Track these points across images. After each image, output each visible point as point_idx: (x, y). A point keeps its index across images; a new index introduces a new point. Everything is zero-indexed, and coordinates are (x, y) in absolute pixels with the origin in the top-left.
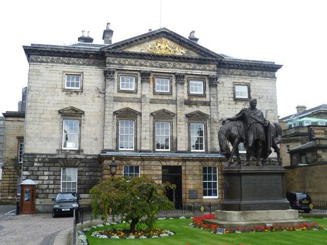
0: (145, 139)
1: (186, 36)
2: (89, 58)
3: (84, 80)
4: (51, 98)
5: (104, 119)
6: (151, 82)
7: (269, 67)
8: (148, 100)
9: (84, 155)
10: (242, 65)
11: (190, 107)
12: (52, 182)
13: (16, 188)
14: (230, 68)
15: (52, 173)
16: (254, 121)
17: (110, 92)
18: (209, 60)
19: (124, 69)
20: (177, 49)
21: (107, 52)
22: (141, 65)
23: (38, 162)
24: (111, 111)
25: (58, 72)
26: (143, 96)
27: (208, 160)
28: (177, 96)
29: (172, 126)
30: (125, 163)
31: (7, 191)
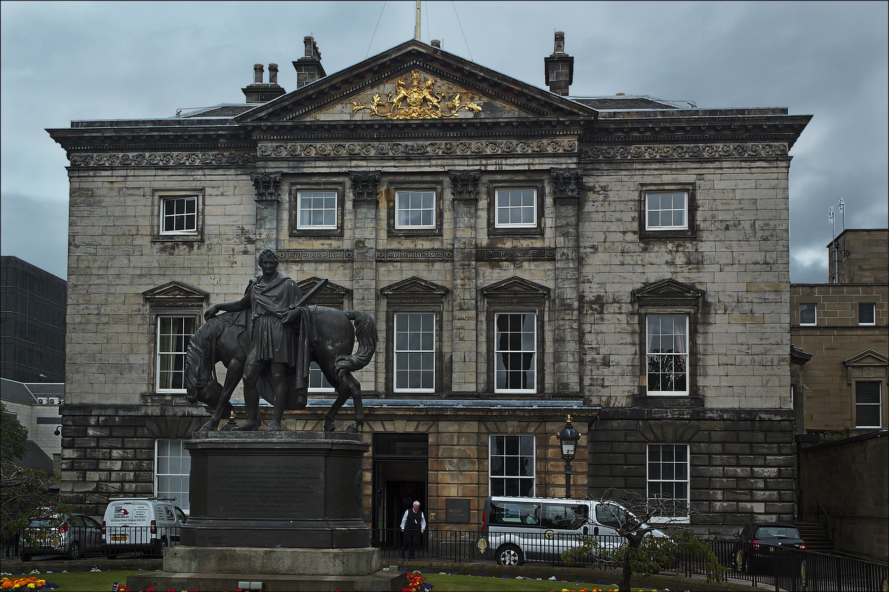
4: (126, 261)
6: (383, 205)
8: (371, 253)
11: (493, 267)
19: (306, 170)
20: (457, 102)
22: (352, 157)
25: (141, 192)
26: (360, 244)
28: (455, 238)
29: (440, 323)
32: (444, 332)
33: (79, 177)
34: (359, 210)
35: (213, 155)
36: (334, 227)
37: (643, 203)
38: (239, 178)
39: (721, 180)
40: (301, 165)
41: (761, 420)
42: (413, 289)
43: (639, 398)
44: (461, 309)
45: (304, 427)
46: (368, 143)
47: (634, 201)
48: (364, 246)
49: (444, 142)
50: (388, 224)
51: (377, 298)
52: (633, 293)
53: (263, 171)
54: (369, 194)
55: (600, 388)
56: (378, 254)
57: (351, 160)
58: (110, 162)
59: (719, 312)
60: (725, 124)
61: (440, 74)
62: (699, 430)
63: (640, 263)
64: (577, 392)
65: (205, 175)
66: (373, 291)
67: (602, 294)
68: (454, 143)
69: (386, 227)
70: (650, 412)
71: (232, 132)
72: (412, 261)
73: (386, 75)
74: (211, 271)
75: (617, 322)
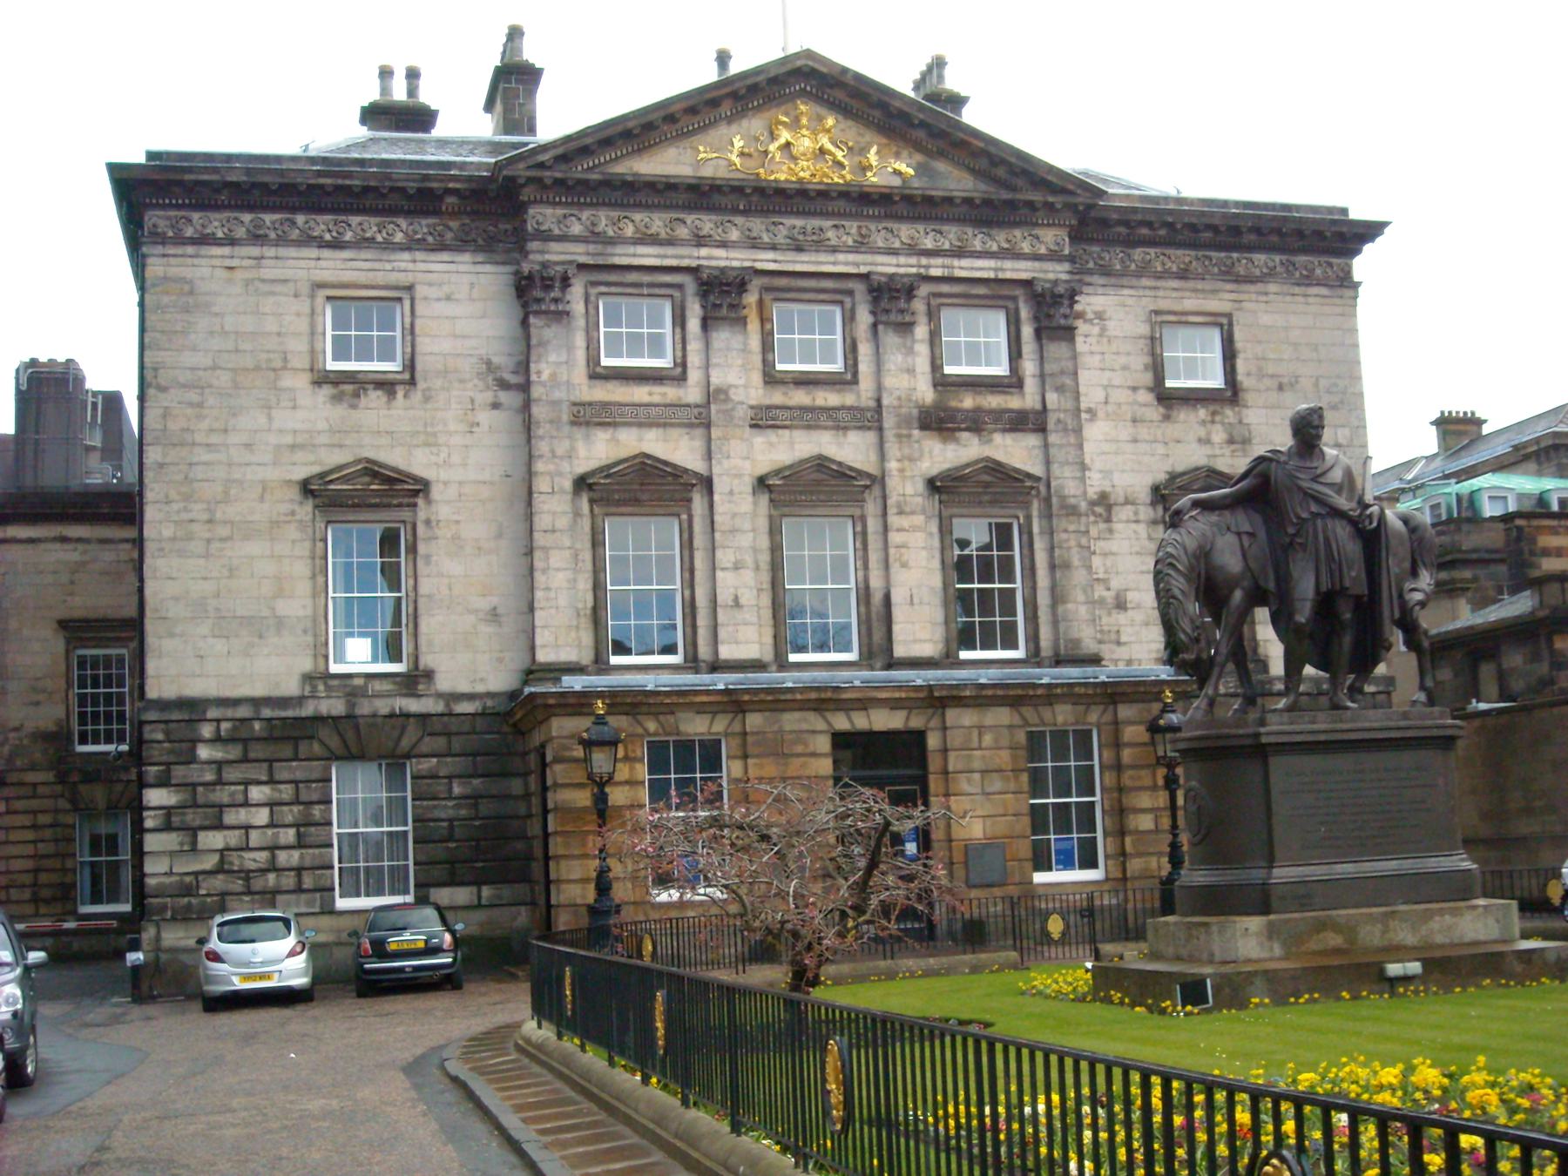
0: (737, 603)
1: (900, 78)
2: (436, 213)
3: (418, 322)
4: (262, 420)
5: (529, 517)
7: (1319, 234)
8: (742, 413)
9: (440, 695)
10: (1193, 228)
11: (945, 440)
12: (289, 836)
13: (68, 879)
14: (1131, 243)
15: (287, 792)
16: (1314, 508)
17: (553, 376)
18: (1030, 205)
19: (618, 261)
20: (872, 157)
21: (530, 180)
22: (700, 240)
23: (217, 739)
24: (560, 474)
27: (1052, 695)
30: (652, 726)
31: (27, 895)
33: (164, 256)
35: (428, 226)
36: (664, 362)
38: (480, 268)
40: (609, 250)
44: (901, 513)
45: (710, 727)
46: (727, 218)
47: (1145, 338)
48: (727, 399)
49: (855, 224)
50: (764, 361)
52: (1156, 489)
53: (539, 258)
54: (732, 307)
55: (1114, 647)
56: (750, 413)
57: (699, 245)
58: (226, 230)
60: (1275, 225)
61: (845, 109)
63: (1160, 437)
65: (414, 261)
67: (1108, 489)
68: (873, 227)
69: (759, 364)
71: (474, 186)
72: (809, 427)
74: (431, 440)
75: (1133, 535)
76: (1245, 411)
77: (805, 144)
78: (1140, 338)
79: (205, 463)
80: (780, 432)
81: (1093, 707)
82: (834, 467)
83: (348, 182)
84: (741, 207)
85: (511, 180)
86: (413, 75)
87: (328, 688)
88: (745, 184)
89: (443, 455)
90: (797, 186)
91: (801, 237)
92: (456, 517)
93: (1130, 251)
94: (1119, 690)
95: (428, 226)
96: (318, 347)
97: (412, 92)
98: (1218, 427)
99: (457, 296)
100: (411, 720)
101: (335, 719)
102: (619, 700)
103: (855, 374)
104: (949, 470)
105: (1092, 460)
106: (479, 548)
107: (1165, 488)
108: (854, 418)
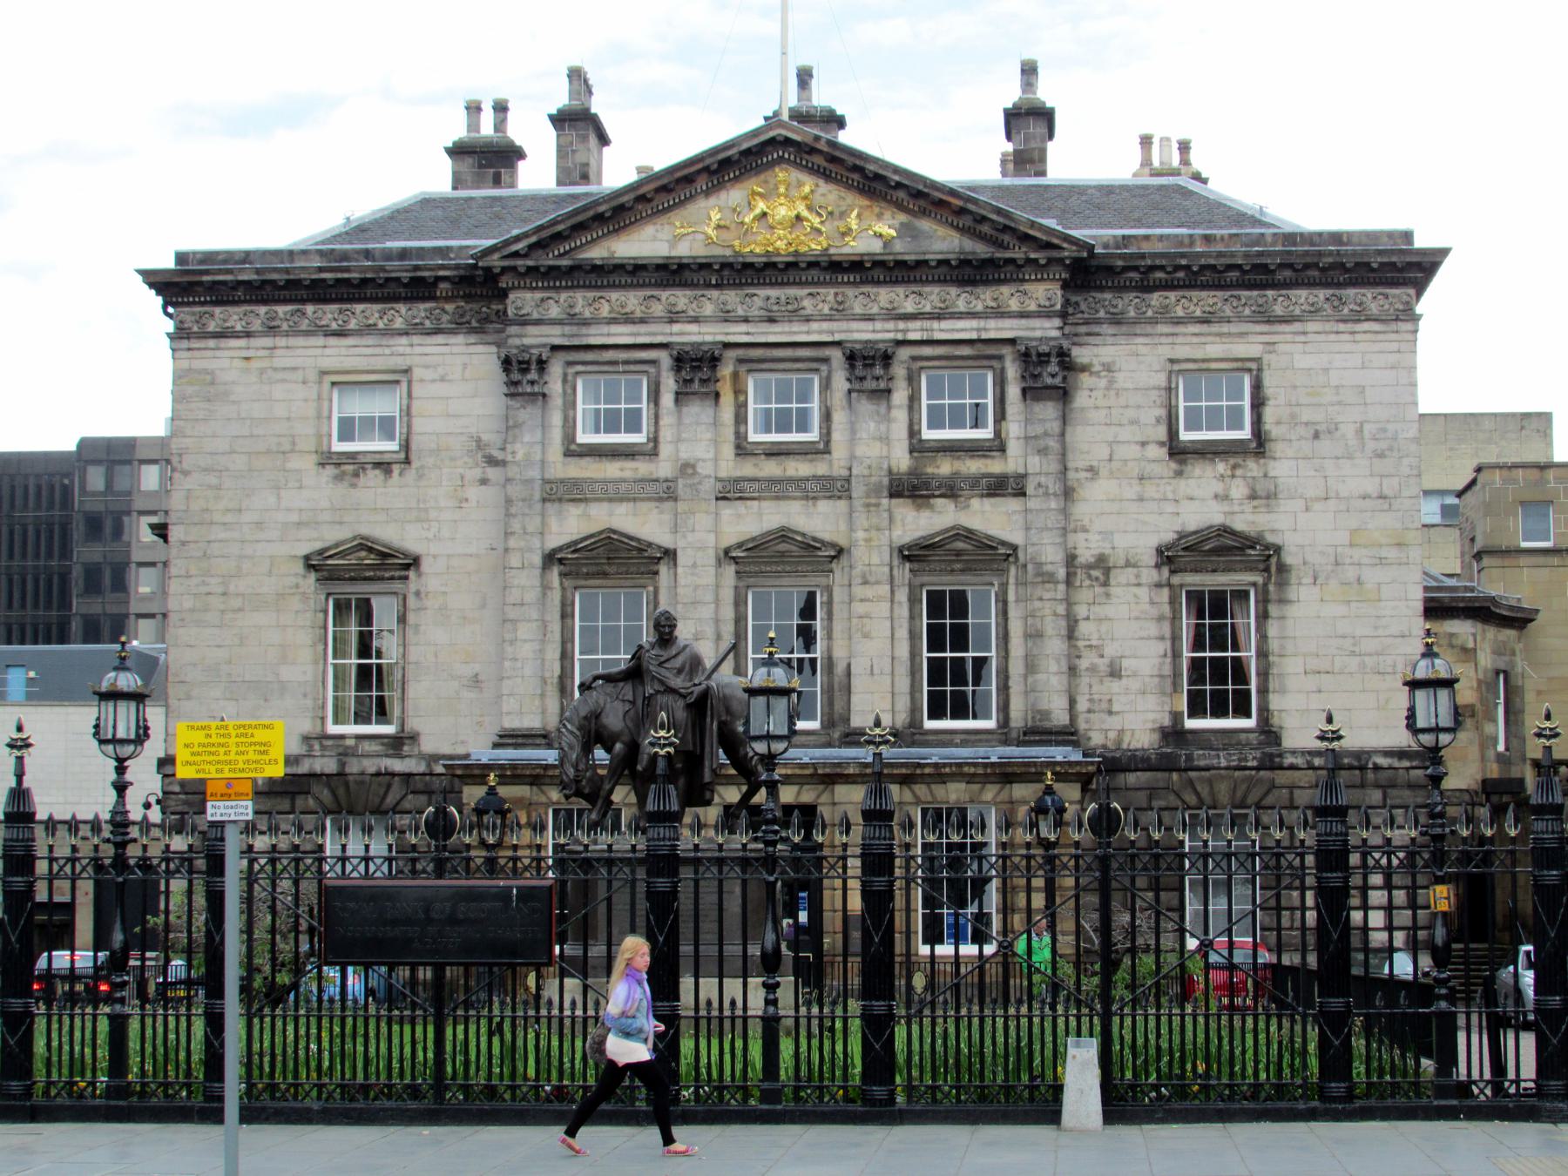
3: (416, 405)
4: (272, 500)
6: (727, 399)
8: (709, 487)
9: (422, 756)
11: (919, 507)
14: (1147, 288)
18: (1012, 261)
21: (504, 270)
22: (673, 317)
24: (530, 550)
25: (299, 376)
26: (687, 468)
28: (852, 457)
32: (835, 623)
33: (189, 349)
34: (685, 410)
35: (426, 310)
37: (1173, 392)
39: (1305, 353)
40: (584, 330)
41: (1377, 768)
42: (783, 547)
43: (1174, 734)
44: (865, 583)
46: (700, 293)
48: (695, 473)
49: (832, 291)
51: (719, 563)
53: (517, 341)
54: (704, 381)
55: (1105, 716)
56: (719, 486)
57: (672, 321)
58: (244, 323)
59: (1305, 581)
62: (1273, 786)
63: (1170, 496)
64: (1065, 726)
65: (412, 345)
66: (711, 553)
67: (1107, 552)
68: (850, 292)
69: (731, 437)
70: (1189, 758)
71: (462, 272)
72: (777, 498)
73: (732, 175)
76: (1272, 463)
77: (782, 212)
78: (1154, 388)
79: (221, 541)
80: (749, 503)
81: (989, 786)
82: (799, 538)
83: (346, 275)
84: (714, 282)
85: (488, 270)
86: (501, 108)
87: (323, 748)
88: (712, 260)
89: (434, 530)
90: (764, 260)
91: (775, 308)
92: (443, 589)
93: (1146, 296)
94: (1010, 770)
95: (426, 310)
96: (325, 430)
97: (500, 125)
98: (1238, 481)
99: (450, 377)
100: (396, 778)
101: (328, 775)
102: (519, 772)
103: (828, 443)
104: (924, 538)
105: (1091, 521)
106: (465, 618)
107: (1168, 549)
108: (824, 488)
